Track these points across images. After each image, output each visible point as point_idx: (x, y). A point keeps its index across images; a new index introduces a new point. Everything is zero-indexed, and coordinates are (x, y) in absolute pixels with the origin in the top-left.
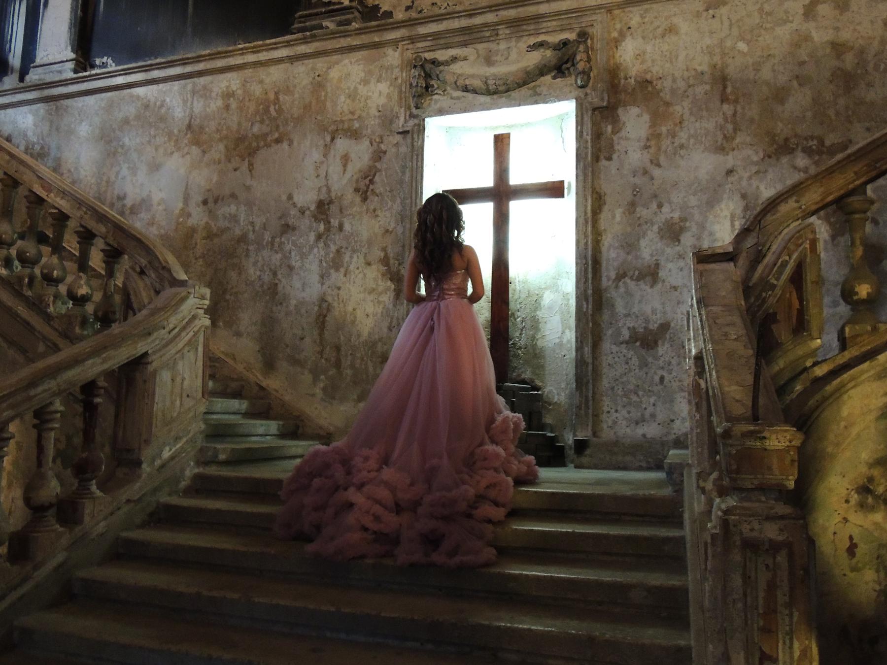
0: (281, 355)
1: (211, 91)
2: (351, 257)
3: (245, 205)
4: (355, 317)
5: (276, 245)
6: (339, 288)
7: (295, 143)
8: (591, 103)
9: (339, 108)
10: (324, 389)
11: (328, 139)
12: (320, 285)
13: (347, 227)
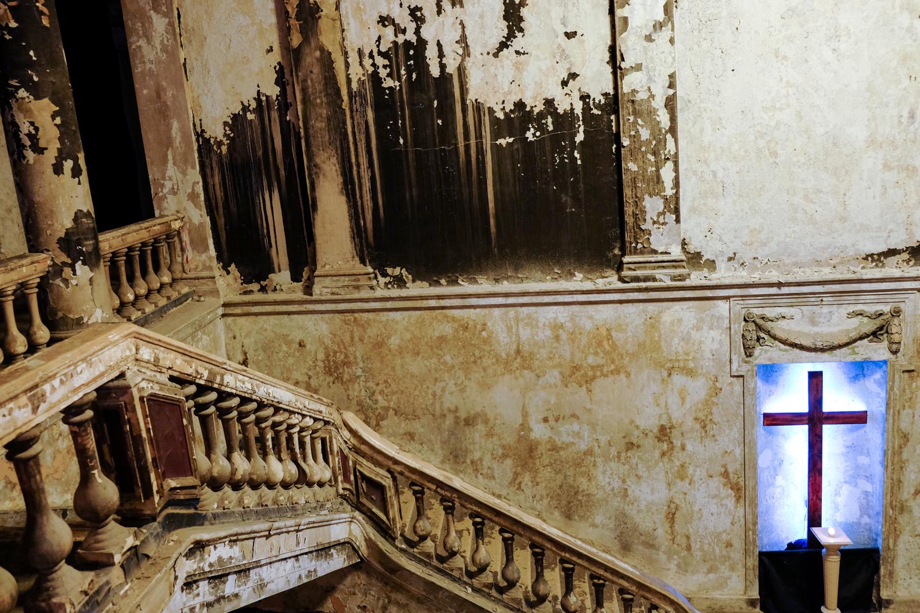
0: (636, 541)
1: (537, 321)
2: (694, 471)
3: (588, 425)
4: (702, 515)
5: (623, 458)
6: (685, 494)
7: (632, 375)
8: (901, 366)
9: (673, 348)
10: (678, 566)
11: (665, 374)
12: (667, 491)
13: (689, 447)
